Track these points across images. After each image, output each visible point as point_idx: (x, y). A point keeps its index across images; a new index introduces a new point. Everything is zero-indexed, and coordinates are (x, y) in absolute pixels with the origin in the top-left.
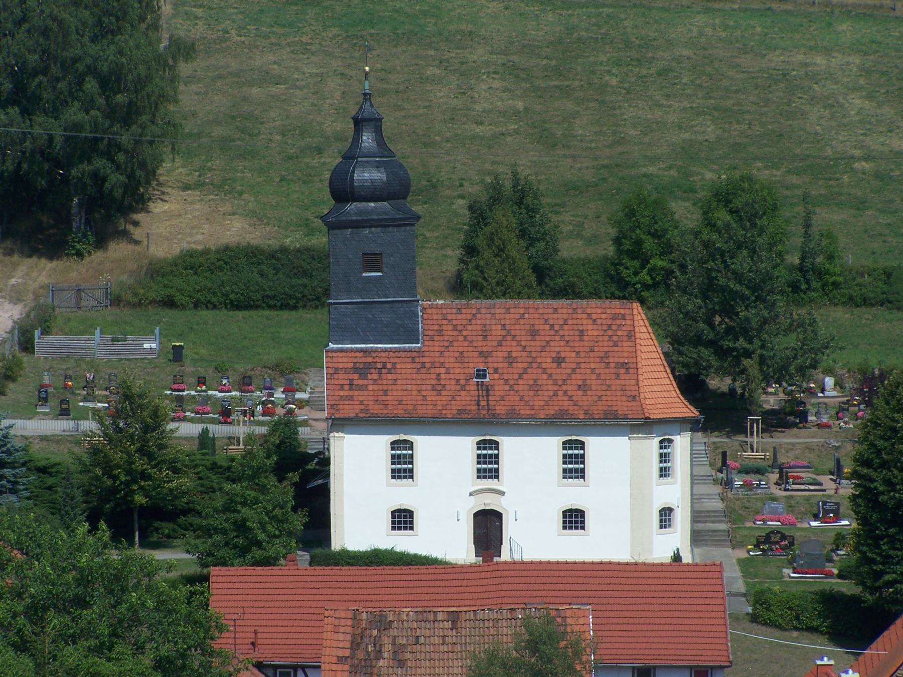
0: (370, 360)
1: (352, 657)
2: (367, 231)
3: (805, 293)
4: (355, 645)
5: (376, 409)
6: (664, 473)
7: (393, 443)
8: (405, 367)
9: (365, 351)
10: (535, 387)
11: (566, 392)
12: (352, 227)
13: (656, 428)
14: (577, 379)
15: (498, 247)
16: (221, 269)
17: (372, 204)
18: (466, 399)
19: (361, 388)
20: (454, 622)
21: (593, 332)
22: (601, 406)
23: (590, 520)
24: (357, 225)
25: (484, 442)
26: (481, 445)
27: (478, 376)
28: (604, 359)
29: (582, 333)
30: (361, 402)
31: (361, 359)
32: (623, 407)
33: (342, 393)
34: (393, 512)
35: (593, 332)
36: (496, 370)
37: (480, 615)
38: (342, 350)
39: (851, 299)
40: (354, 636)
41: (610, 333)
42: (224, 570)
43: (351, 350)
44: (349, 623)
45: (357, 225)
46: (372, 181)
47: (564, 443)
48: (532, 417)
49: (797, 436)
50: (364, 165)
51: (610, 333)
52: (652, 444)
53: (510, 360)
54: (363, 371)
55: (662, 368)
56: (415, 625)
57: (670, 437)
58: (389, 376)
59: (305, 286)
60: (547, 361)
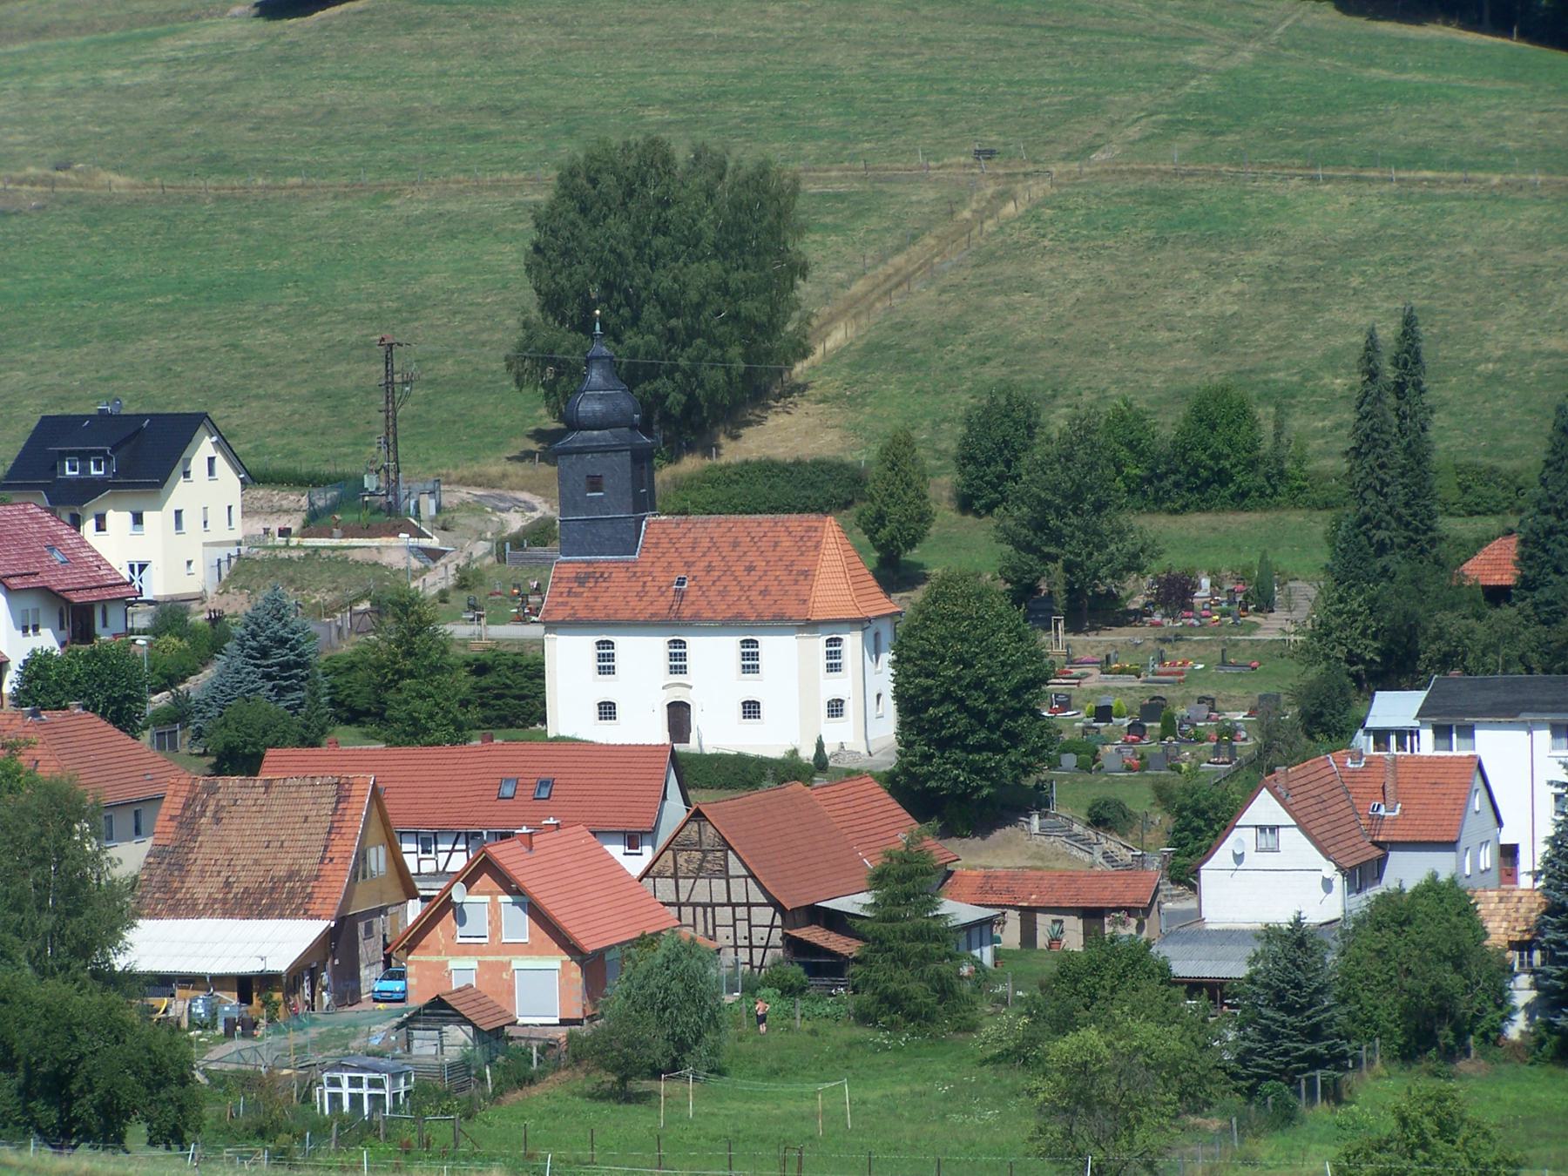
0: (591, 570)
1: (182, 816)
2: (589, 456)
3: (1271, 497)
4: (186, 806)
5: (582, 614)
6: (833, 668)
7: (598, 643)
8: (619, 576)
9: (589, 562)
10: (723, 593)
11: (748, 597)
12: (578, 453)
13: (820, 627)
14: (761, 585)
15: (892, 462)
16: (737, 482)
17: (596, 433)
18: (662, 606)
19: (577, 595)
20: (267, 788)
21: (786, 542)
22: (775, 609)
23: (824, 709)
24: (580, 451)
25: (675, 641)
26: (745, 643)
27: (678, 584)
28: (789, 569)
29: (776, 544)
30: (573, 608)
31: (583, 569)
32: (792, 609)
33: (560, 600)
34: (600, 704)
35: (786, 542)
36: (694, 578)
37: (289, 782)
38: (569, 562)
39: (1314, 502)
40: (188, 799)
41: (800, 544)
42: (277, 751)
43: (578, 562)
44: (187, 788)
45: (580, 451)
46: (594, 412)
47: (670, 642)
48: (711, 620)
49: (1119, 634)
50: (589, 398)
51: (800, 544)
52: (819, 643)
53: (709, 569)
54: (581, 580)
55: (842, 575)
56: (237, 790)
57: (754, 638)
58: (604, 584)
59: (809, 498)
60: (739, 569)
